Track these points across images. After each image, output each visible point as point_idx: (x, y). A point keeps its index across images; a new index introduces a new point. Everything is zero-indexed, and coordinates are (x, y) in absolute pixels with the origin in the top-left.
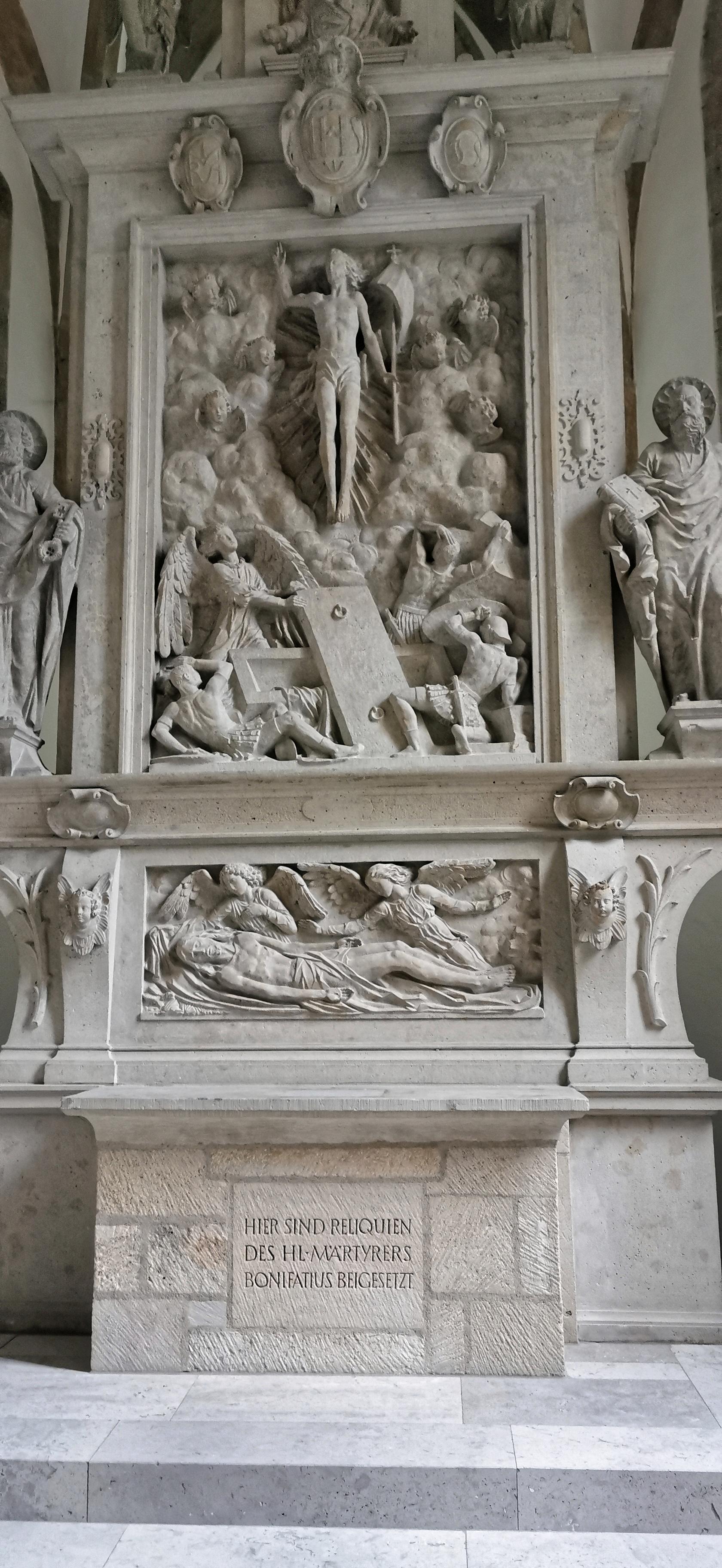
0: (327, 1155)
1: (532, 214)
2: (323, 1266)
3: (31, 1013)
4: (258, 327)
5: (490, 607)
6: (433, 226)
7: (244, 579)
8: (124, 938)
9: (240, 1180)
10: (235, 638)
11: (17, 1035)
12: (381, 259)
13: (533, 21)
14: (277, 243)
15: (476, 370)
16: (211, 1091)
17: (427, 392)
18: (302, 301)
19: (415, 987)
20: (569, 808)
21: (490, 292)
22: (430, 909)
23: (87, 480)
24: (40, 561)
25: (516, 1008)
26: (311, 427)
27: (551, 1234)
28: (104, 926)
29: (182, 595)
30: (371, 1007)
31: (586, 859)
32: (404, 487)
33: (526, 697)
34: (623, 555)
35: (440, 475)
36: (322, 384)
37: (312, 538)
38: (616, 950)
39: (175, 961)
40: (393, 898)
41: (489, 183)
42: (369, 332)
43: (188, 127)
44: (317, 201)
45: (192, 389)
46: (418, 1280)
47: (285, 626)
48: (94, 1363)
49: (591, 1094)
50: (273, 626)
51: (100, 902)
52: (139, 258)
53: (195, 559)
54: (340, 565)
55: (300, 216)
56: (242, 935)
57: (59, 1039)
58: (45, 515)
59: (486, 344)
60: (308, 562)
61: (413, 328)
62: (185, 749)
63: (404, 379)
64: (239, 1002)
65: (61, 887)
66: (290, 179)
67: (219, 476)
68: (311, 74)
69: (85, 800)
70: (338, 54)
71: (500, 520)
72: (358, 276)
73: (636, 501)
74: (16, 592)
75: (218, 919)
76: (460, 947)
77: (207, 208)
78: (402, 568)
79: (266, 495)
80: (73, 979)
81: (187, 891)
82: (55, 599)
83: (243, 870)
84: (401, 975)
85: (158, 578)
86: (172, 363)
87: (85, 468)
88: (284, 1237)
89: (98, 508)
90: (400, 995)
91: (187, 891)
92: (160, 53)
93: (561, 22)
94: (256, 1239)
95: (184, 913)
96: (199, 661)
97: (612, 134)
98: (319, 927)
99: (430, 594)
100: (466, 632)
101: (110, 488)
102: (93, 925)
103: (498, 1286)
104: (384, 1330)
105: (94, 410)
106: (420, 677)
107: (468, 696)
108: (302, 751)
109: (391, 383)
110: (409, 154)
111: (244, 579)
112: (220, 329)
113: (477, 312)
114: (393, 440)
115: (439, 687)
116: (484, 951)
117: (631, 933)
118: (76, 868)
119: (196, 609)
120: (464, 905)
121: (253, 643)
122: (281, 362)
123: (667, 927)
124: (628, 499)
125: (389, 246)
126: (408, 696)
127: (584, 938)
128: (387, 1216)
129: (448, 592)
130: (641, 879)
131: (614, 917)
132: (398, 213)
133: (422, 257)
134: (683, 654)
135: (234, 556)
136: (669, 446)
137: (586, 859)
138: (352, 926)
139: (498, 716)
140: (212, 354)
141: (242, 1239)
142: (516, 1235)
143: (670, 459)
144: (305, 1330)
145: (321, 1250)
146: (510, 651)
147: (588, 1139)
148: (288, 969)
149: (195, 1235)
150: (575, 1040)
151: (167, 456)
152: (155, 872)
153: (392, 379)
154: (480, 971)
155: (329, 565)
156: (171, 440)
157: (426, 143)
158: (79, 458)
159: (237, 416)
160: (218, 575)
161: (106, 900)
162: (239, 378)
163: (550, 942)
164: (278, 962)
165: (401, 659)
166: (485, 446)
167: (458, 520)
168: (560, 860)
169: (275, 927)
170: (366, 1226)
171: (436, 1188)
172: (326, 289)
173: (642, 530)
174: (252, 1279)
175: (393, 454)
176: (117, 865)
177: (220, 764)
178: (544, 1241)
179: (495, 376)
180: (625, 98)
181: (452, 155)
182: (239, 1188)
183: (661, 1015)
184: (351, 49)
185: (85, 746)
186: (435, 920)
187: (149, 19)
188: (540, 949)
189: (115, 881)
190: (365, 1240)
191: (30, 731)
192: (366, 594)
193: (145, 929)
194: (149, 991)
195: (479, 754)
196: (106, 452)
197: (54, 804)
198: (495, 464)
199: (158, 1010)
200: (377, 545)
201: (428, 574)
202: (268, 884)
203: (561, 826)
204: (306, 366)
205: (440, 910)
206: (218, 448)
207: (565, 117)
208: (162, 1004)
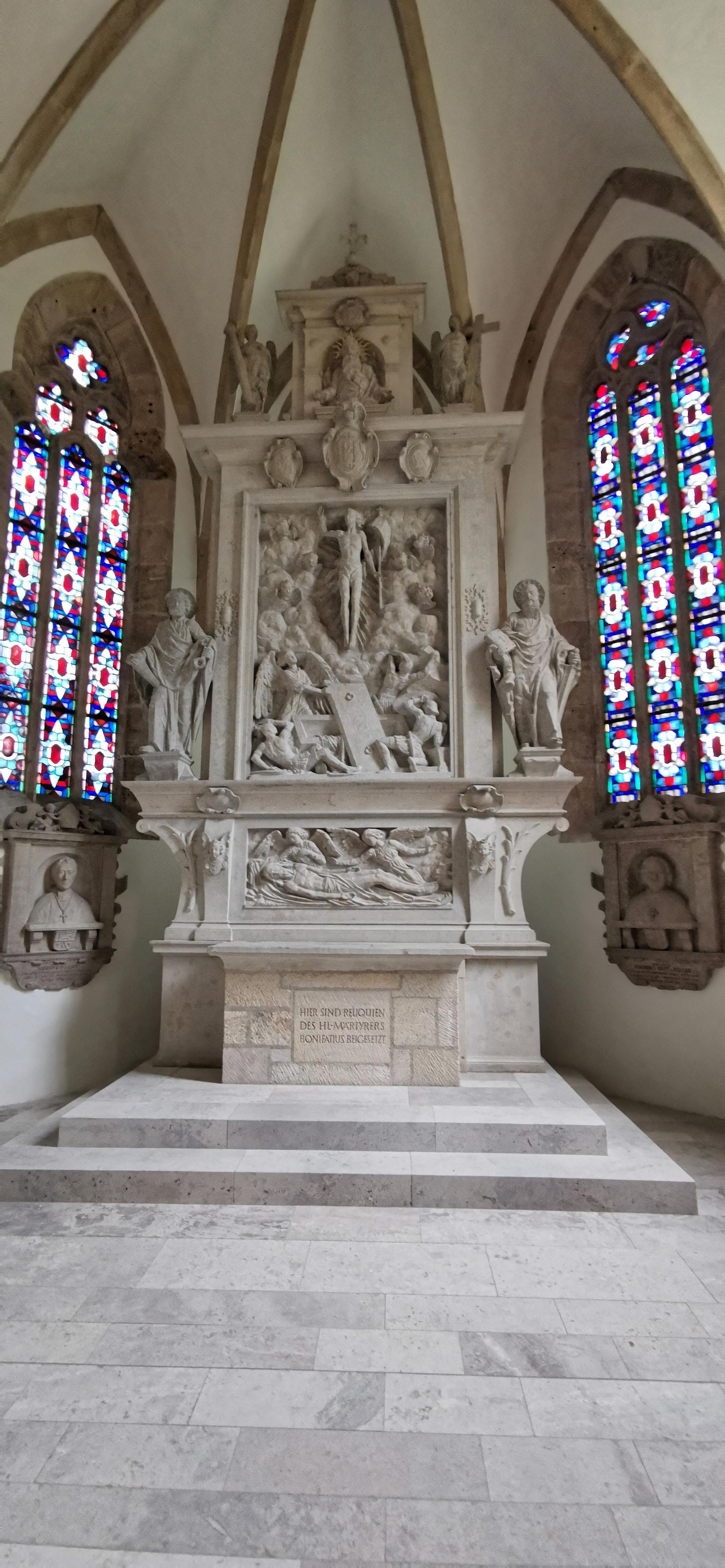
0: (342, 976)
1: (452, 493)
2: (339, 1032)
3: (188, 903)
5: (428, 695)
6: (402, 498)
7: (300, 678)
8: (236, 865)
9: (297, 989)
10: (295, 709)
11: (179, 916)
12: (374, 513)
13: (454, 392)
14: (319, 505)
15: (422, 572)
16: (283, 945)
17: (397, 583)
18: (332, 534)
19: (387, 892)
20: (467, 801)
21: (430, 531)
22: (395, 853)
23: (219, 625)
24: (194, 668)
25: (439, 903)
26: (336, 599)
27: (455, 1016)
28: (226, 859)
29: (267, 686)
30: (364, 902)
31: (476, 828)
32: (384, 632)
33: (446, 743)
34: (498, 671)
35: (403, 627)
36: (342, 578)
37: (336, 658)
38: (490, 874)
39: (262, 878)
40: (376, 847)
41: (430, 476)
42: (367, 551)
43: (274, 444)
44: (341, 484)
45: (274, 578)
46: (387, 1039)
47: (321, 703)
48: (224, 1079)
49: (477, 948)
50: (315, 703)
51: (224, 847)
52: (247, 510)
53: (275, 668)
54: (350, 672)
55: (332, 491)
56: (298, 865)
57: (202, 918)
58: (196, 644)
59: (428, 558)
60: (334, 670)
61: (390, 548)
62: (268, 767)
63: (384, 575)
64: (296, 899)
65: (204, 839)
66: (327, 471)
67: (288, 624)
68: (338, 420)
69: (216, 794)
70: (353, 411)
71: (433, 650)
72: (362, 522)
73: (504, 643)
74: (180, 684)
75: (285, 856)
76: (410, 872)
77: (283, 486)
78: (382, 674)
79: (312, 634)
80: (209, 886)
81: (269, 842)
82: (201, 688)
83: (298, 831)
84: (380, 886)
85: (255, 678)
86: (263, 564)
87: (217, 619)
88: (320, 1018)
89: (224, 640)
90: (379, 896)
91: (269, 842)
92: (259, 402)
93: (468, 393)
94: (305, 1018)
95: (267, 853)
96: (277, 721)
97: (494, 453)
98: (338, 861)
99: (397, 688)
100: (416, 709)
101: (231, 629)
102: (220, 859)
103: (427, 1042)
104: (370, 1064)
105: (223, 589)
106: (391, 731)
107: (416, 742)
108: (329, 769)
109: (378, 577)
110: (388, 460)
111: (300, 678)
112: (289, 547)
113: (423, 542)
114: (379, 607)
115: (401, 737)
116: (423, 874)
117: (498, 866)
118: (212, 829)
119: (274, 694)
120: (413, 850)
121: (305, 712)
122: (320, 565)
123: (517, 863)
124: (500, 642)
125: (378, 507)
126: (385, 742)
127: (474, 868)
128: (372, 1007)
129: (406, 687)
130: (504, 838)
131: (490, 857)
132: (383, 490)
133: (394, 513)
134: (527, 722)
135: (295, 667)
136: (521, 614)
137: (476, 828)
138: (355, 861)
139: (431, 752)
140: (285, 560)
141: (299, 1019)
142: (437, 1017)
143: (522, 621)
144: (330, 1064)
145: (338, 1024)
146: (438, 718)
147: (474, 971)
148: (321, 883)
149: (275, 1017)
150: (469, 920)
151: (260, 612)
152: (253, 832)
153: (379, 575)
154: (420, 884)
155: (344, 671)
156: (263, 604)
157: (398, 455)
158: (214, 613)
159: (297, 593)
160: (287, 678)
161: (227, 845)
162: (299, 572)
163: (457, 870)
164: (316, 879)
165: (382, 722)
166: (425, 611)
167: (412, 650)
168: (462, 828)
169: (314, 861)
170: (362, 1012)
171: (396, 994)
172: (345, 528)
173: (507, 658)
174: (304, 1038)
175: (379, 615)
176: (232, 827)
177: (286, 775)
178: (451, 1020)
179: (432, 575)
180: (501, 435)
181: (411, 462)
182: (297, 993)
183: (512, 908)
184: (360, 407)
185: (216, 765)
186: (398, 859)
187: (254, 384)
188: (452, 873)
189: (232, 835)
190: (361, 1020)
191: (187, 756)
192: (364, 687)
193: (247, 861)
194: (249, 893)
195: (422, 773)
196: (229, 611)
197: (200, 795)
198: (431, 621)
199: (253, 903)
200: (370, 662)
201: (396, 678)
202: (313, 837)
203: (464, 811)
204: (333, 567)
205: (401, 853)
206: (287, 610)
207: (469, 444)
208: (256, 900)
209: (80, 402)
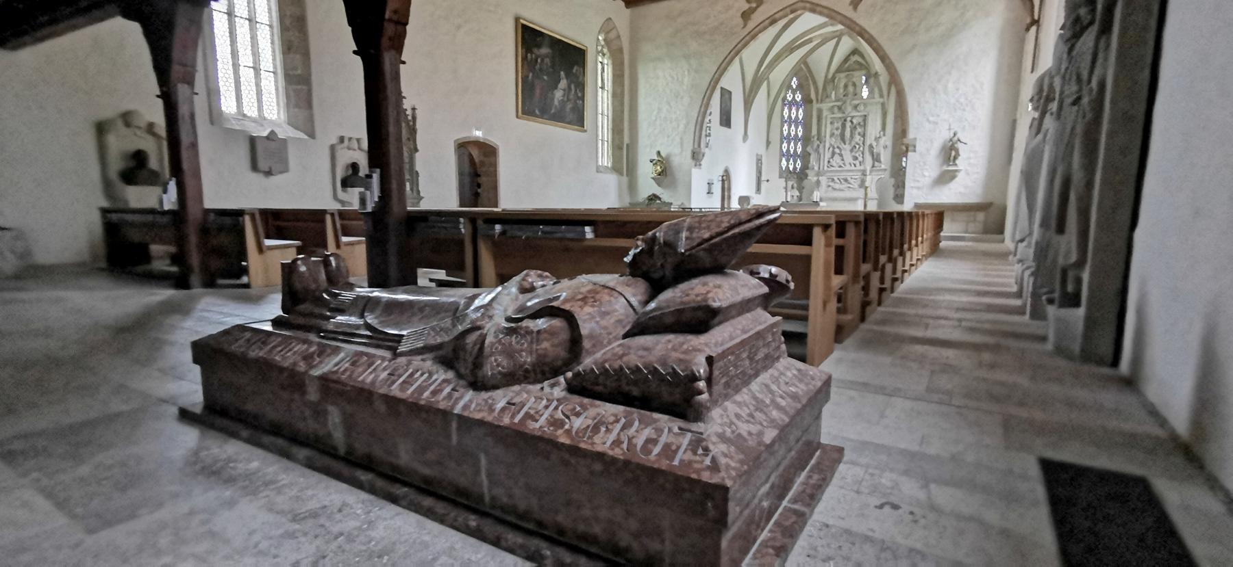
4: (839, 125)
7: (837, 151)
68: (845, 102)
73: (874, 144)
110: (856, 107)
111: (837, 151)
195: (858, 167)
209: (794, 93)
